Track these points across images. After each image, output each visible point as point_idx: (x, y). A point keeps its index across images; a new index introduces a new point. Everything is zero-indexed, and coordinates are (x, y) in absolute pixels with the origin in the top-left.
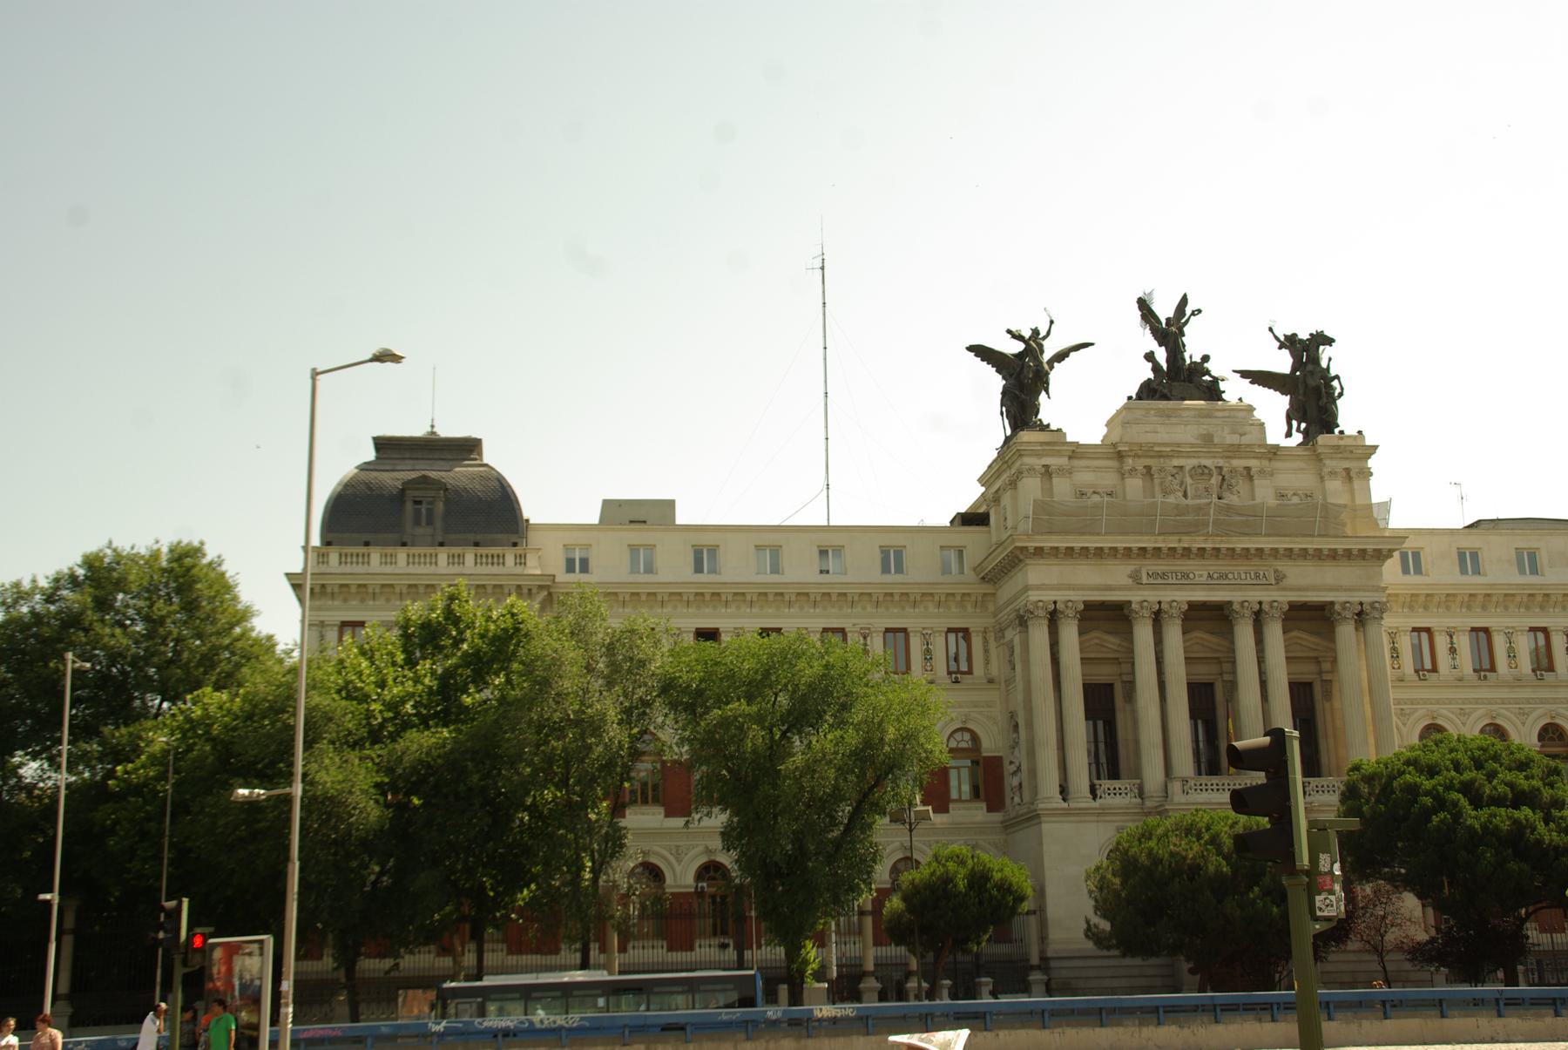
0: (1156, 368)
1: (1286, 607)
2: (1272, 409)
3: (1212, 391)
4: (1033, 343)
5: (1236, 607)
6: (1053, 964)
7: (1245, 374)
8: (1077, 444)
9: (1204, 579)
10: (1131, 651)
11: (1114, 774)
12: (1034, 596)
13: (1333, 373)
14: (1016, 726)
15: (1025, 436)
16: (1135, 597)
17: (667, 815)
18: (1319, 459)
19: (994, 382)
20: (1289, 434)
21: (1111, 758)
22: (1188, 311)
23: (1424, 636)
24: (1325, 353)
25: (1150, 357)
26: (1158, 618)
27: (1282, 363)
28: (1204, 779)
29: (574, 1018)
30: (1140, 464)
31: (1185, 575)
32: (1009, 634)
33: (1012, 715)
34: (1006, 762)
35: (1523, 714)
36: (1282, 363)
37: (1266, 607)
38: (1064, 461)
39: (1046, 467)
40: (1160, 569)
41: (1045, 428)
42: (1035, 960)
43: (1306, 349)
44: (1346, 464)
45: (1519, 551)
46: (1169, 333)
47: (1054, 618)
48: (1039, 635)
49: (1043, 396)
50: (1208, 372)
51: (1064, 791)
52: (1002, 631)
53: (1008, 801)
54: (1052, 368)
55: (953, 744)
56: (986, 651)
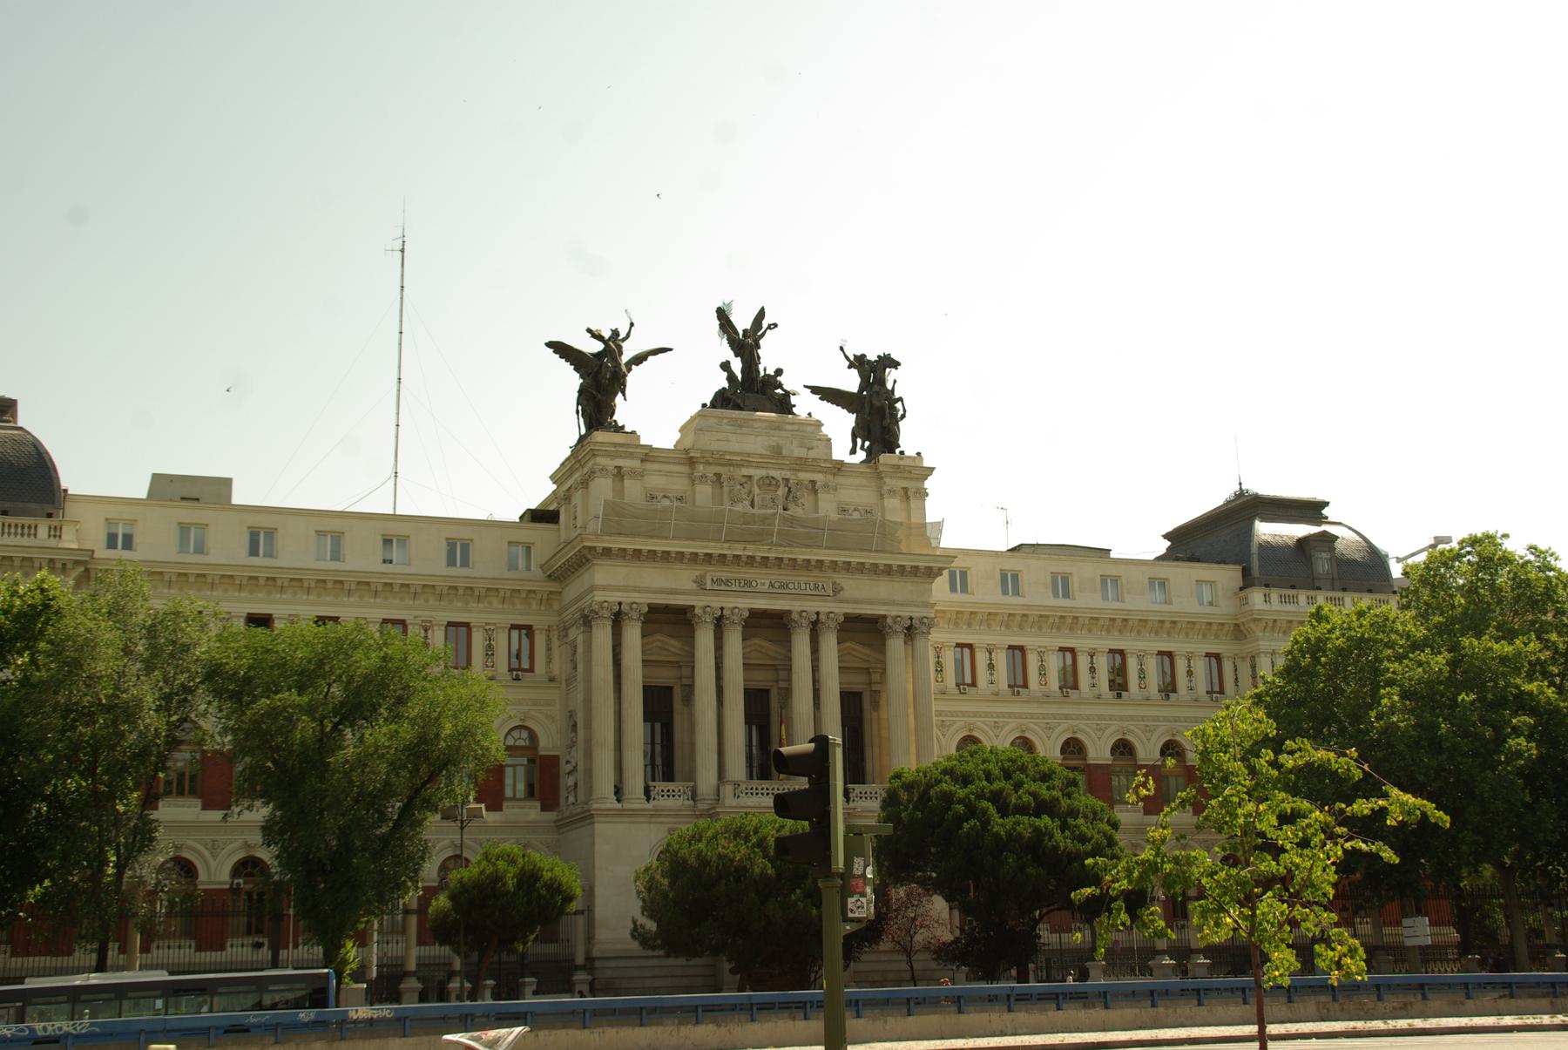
0: (731, 378)
1: (842, 619)
2: (839, 425)
3: (784, 405)
4: (613, 343)
5: (795, 616)
6: (598, 964)
7: (815, 390)
8: (650, 447)
9: (765, 588)
10: (692, 655)
11: (669, 776)
12: (599, 596)
13: (897, 395)
14: (575, 726)
15: (600, 436)
16: (698, 602)
17: (204, 808)
18: (880, 477)
19: (571, 380)
20: (853, 452)
21: (666, 760)
22: (765, 324)
23: (967, 651)
24: (891, 375)
25: (725, 366)
26: (719, 623)
27: (850, 382)
28: (755, 783)
29: (85, 1024)
30: (711, 471)
31: (748, 583)
32: (573, 633)
33: (572, 714)
34: (563, 762)
35: (1050, 728)
36: (850, 382)
37: (823, 618)
38: (636, 464)
39: (619, 468)
40: (724, 575)
41: (619, 429)
42: (580, 960)
43: (874, 370)
44: (905, 484)
45: (1054, 575)
46: (746, 345)
47: (618, 619)
48: (602, 635)
49: (619, 398)
50: (780, 386)
51: (618, 792)
52: (566, 629)
53: (562, 800)
54: (629, 370)
55: (510, 742)
56: (549, 649)
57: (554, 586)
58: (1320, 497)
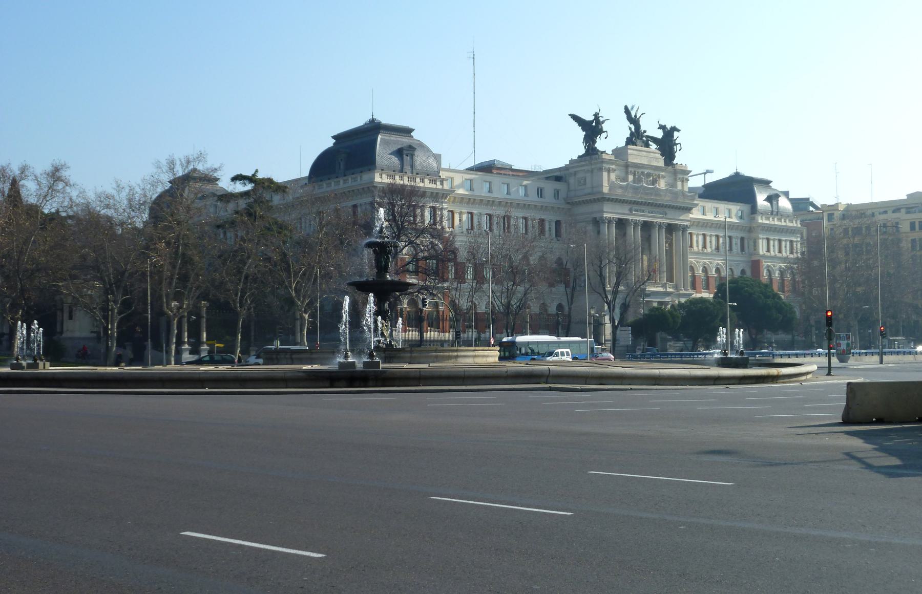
13: (677, 142)
24: (676, 134)
25: (630, 129)
27: (659, 134)
36: (659, 134)
46: (634, 121)
57: (569, 206)
58: (770, 179)
